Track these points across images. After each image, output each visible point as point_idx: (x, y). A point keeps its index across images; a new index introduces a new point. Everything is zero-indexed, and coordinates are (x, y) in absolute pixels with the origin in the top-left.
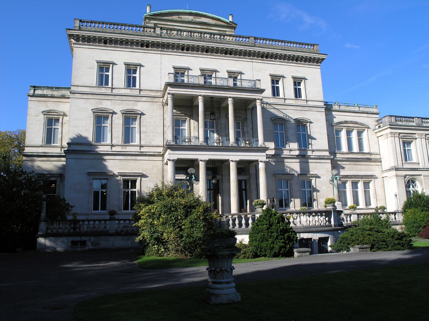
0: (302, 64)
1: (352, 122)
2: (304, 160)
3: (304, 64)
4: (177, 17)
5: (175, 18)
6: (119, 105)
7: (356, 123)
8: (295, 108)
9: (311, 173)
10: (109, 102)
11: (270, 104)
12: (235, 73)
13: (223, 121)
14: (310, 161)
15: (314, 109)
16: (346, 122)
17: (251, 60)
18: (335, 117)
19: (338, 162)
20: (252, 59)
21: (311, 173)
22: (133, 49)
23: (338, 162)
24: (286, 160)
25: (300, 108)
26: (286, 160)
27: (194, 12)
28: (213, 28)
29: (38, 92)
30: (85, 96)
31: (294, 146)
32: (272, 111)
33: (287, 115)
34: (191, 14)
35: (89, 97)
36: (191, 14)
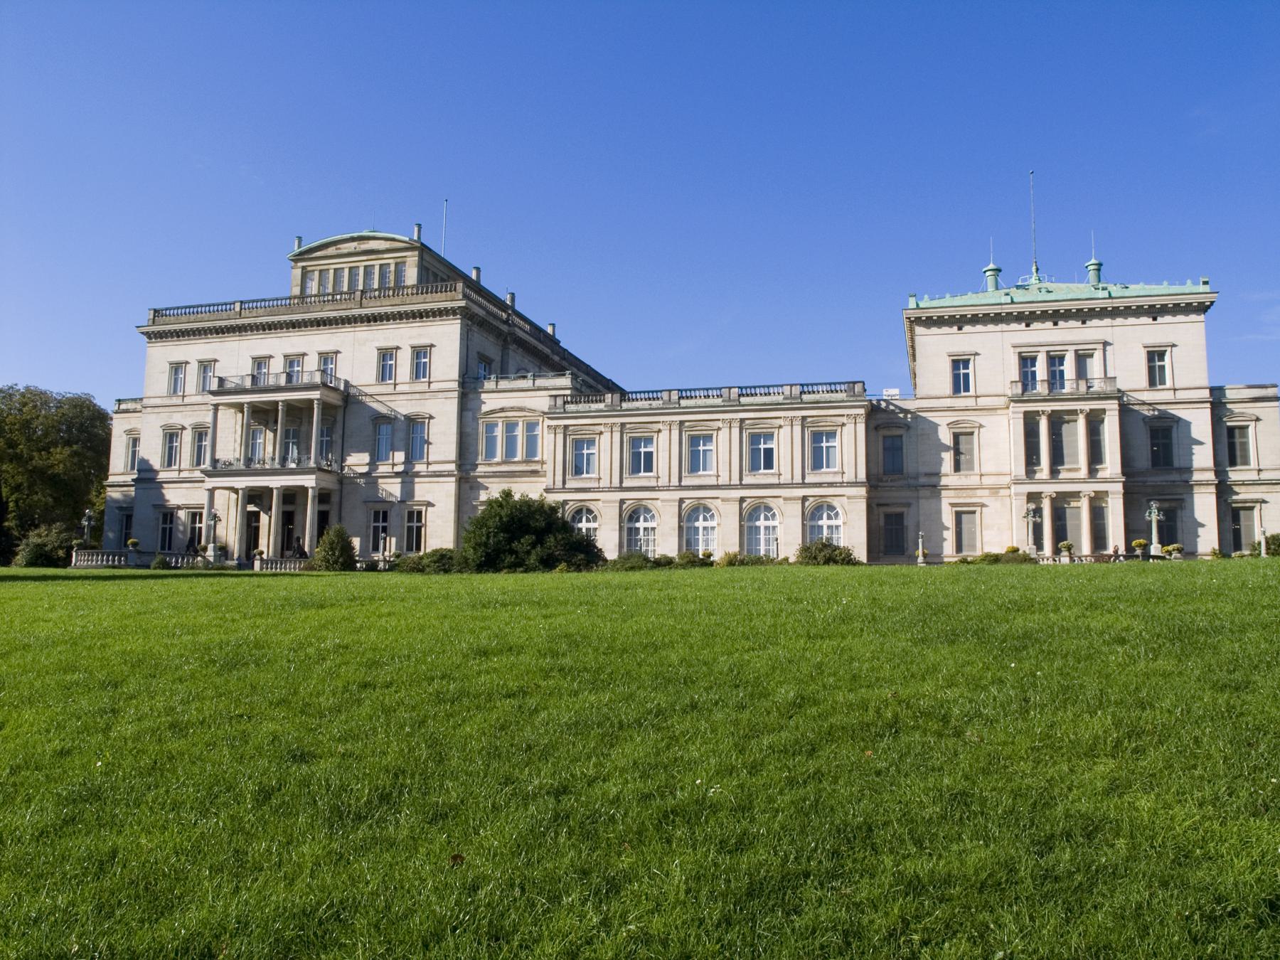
0: (430, 321)
1: (512, 409)
2: (407, 479)
3: (434, 321)
4: (334, 248)
5: (331, 251)
6: (190, 416)
7: (521, 409)
8: (409, 397)
9: (416, 499)
10: (179, 414)
11: (371, 395)
12: (328, 353)
13: (304, 429)
14: (417, 480)
15: (441, 395)
16: (502, 410)
17: (353, 329)
18: (485, 403)
19: (479, 480)
20: (355, 327)
21: (416, 499)
22: (208, 338)
23: (479, 480)
24: (380, 481)
25: (417, 396)
26: (380, 481)
27: (355, 235)
28: (386, 256)
29: (123, 407)
30: (156, 410)
31: (400, 456)
32: (375, 406)
33: (393, 410)
34: (353, 239)
35: (161, 410)
36: (353, 239)
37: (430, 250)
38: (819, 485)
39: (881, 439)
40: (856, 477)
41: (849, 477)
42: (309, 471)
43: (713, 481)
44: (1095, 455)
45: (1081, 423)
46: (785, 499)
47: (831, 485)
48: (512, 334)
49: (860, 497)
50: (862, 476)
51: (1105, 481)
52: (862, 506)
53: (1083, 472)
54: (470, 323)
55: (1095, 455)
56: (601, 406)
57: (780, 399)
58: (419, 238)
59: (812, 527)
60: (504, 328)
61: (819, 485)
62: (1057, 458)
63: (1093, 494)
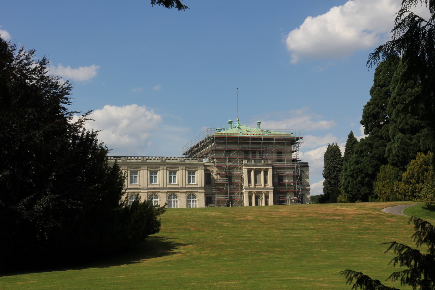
44: (266, 182)
45: (262, 173)
47: (195, 188)
49: (203, 192)
50: (203, 185)
51: (269, 189)
53: (263, 186)
55: (266, 182)
57: (178, 161)
62: (256, 182)
63: (265, 192)
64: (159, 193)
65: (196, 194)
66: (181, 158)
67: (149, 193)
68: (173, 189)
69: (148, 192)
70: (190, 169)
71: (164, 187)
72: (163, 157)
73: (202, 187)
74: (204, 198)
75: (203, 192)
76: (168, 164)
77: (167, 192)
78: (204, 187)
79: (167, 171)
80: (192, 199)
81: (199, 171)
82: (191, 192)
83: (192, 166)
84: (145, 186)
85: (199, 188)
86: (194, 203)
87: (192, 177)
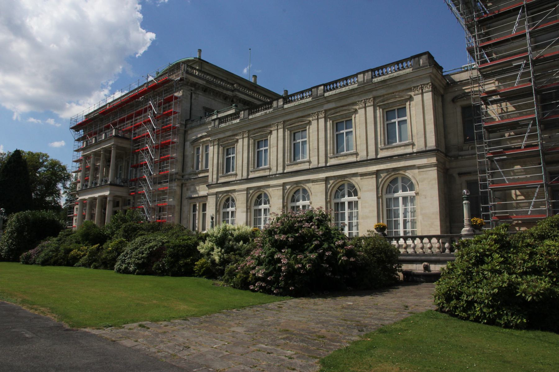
37: (208, 63)
38: (390, 159)
39: (459, 111)
40: (426, 146)
41: (419, 146)
42: (102, 187)
43: (306, 166)
46: (362, 175)
48: (235, 96)
49: (430, 166)
50: (432, 143)
52: (433, 174)
54: (193, 89)
56: (238, 121)
58: (200, 56)
59: (389, 200)
60: (229, 93)
61: (390, 159)
64: (308, 185)
65: (409, 174)
66: (362, 75)
67: (288, 187)
68: (337, 170)
69: (284, 185)
70: (387, 100)
71: (320, 165)
72: (317, 87)
73: (427, 149)
74: (436, 186)
75: (430, 166)
76: (328, 100)
77: (327, 180)
78: (435, 148)
79: (326, 122)
80: (400, 194)
81: (417, 99)
82: (395, 169)
83: (391, 91)
84: (279, 169)
85: (417, 153)
86: (409, 207)
87: (399, 122)
